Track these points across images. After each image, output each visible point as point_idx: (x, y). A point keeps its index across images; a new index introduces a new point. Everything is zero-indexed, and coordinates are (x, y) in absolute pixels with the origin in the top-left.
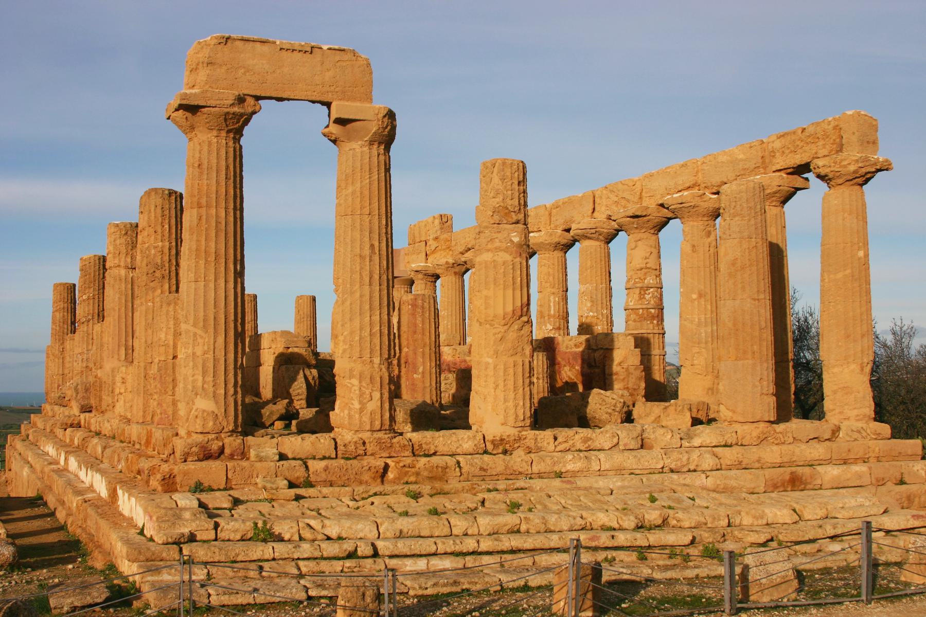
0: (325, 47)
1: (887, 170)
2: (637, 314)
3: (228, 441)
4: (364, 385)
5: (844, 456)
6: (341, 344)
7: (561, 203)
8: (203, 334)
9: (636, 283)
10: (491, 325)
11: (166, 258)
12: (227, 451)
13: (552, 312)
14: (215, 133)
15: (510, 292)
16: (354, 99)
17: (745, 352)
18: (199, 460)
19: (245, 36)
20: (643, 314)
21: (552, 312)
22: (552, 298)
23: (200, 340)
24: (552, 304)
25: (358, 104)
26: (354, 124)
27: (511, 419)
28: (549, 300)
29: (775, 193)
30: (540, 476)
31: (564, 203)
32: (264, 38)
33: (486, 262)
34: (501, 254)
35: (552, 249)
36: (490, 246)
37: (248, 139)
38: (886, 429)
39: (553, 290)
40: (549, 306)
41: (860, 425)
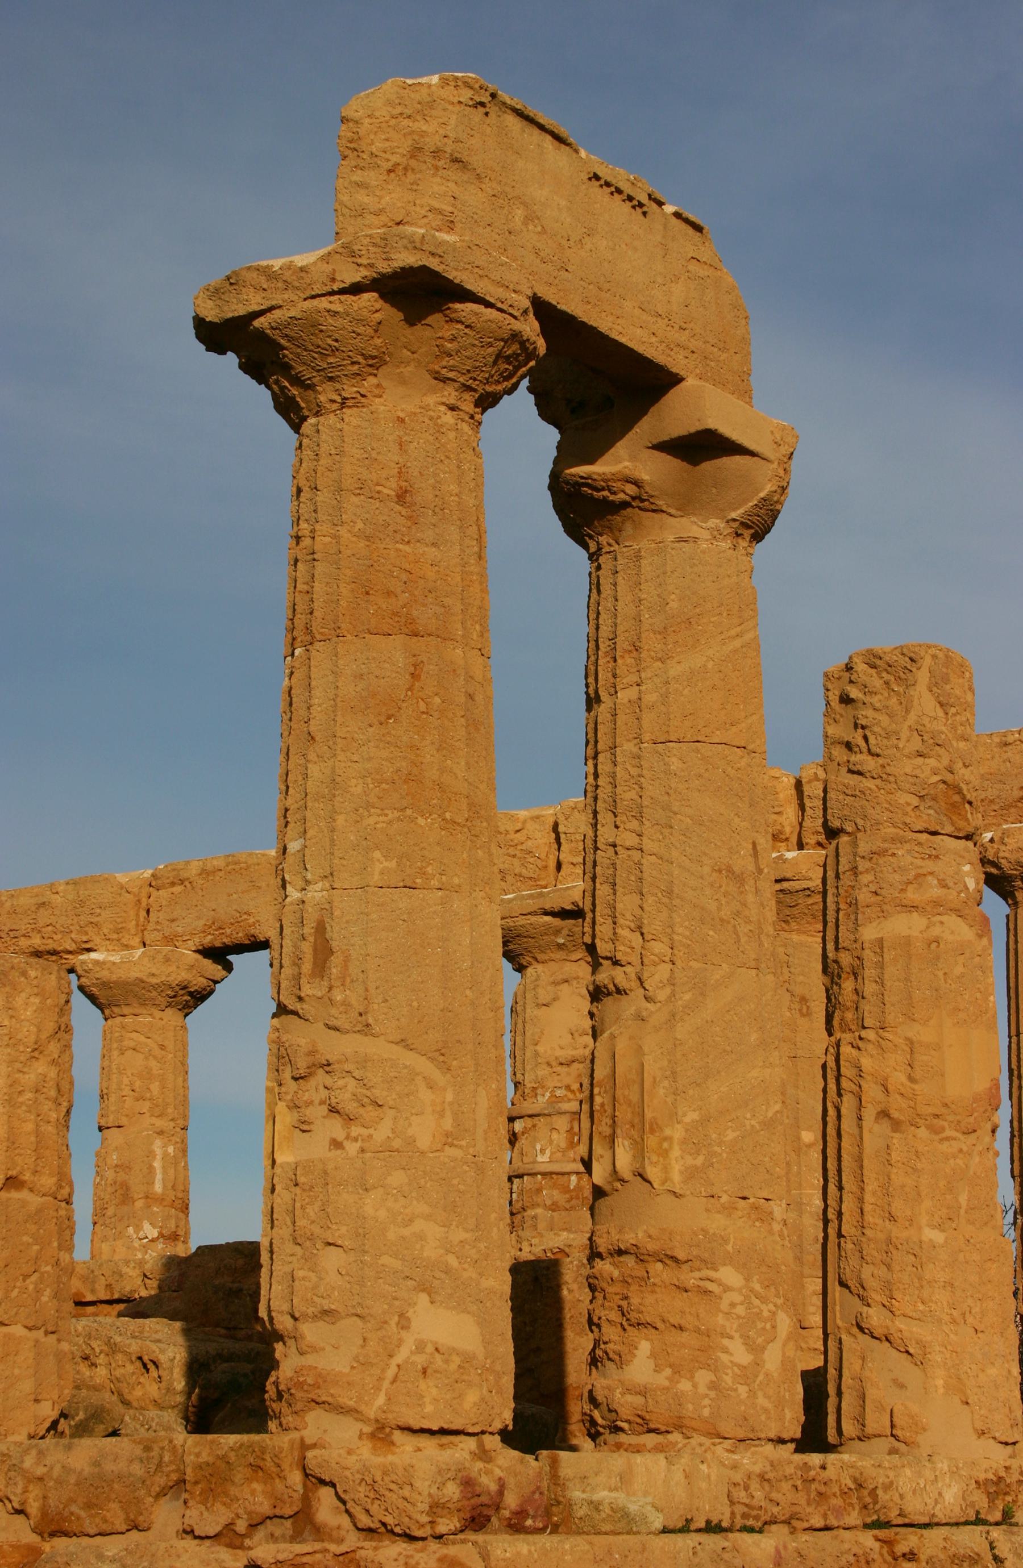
2: (566, 1190)
4: (757, 1287)
6: (676, 1152)
7: (194, 869)
8: (436, 1075)
9: (555, 1099)
10: (935, 1131)
13: (158, 1188)
19: (531, 111)
20: (579, 1188)
21: (158, 1188)
22: (157, 1145)
23: (425, 1095)
24: (157, 1164)
26: (738, 459)
28: (151, 1154)
31: (205, 873)
32: (563, 131)
33: (907, 941)
34: (951, 920)
35: (163, 1001)
36: (912, 895)
39: (160, 1123)
40: (151, 1169)
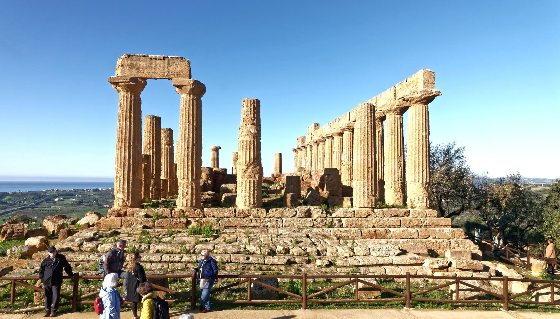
0: (169, 57)
1: (438, 95)
3: (128, 210)
5: (407, 224)
11: (151, 141)
12: (128, 214)
14: (125, 92)
16: (181, 77)
17: (360, 177)
18: (116, 217)
25: (183, 79)
27: (247, 204)
29: (397, 108)
30: (254, 227)
37: (143, 95)
41: (420, 210)
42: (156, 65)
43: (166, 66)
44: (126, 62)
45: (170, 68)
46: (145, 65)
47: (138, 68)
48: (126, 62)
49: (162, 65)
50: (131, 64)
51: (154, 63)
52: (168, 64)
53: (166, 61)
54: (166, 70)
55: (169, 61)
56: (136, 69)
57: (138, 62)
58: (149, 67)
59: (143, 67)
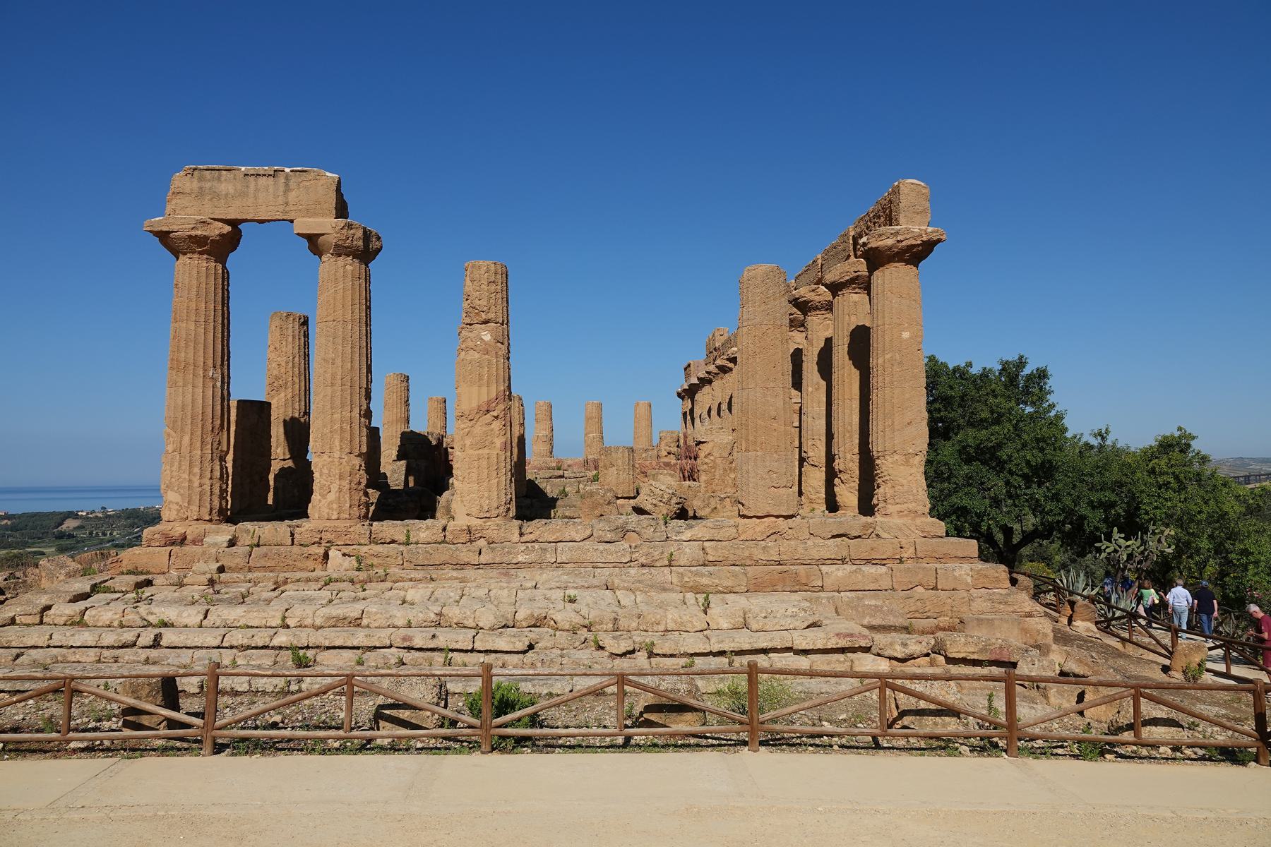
15: (475, 388)
16: (315, 215)
25: (321, 220)
38: (940, 527)
42: (257, 190)
43: (282, 189)
44: (188, 184)
45: (292, 196)
46: (231, 191)
47: (216, 196)
48: (188, 184)
49: (271, 190)
50: (201, 188)
51: (252, 185)
52: (287, 185)
53: (282, 180)
54: (281, 200)
55: (287, 178)
56: (211, 200)
57: (215, 183)
58: (243, 194)
59: (226, 195)
